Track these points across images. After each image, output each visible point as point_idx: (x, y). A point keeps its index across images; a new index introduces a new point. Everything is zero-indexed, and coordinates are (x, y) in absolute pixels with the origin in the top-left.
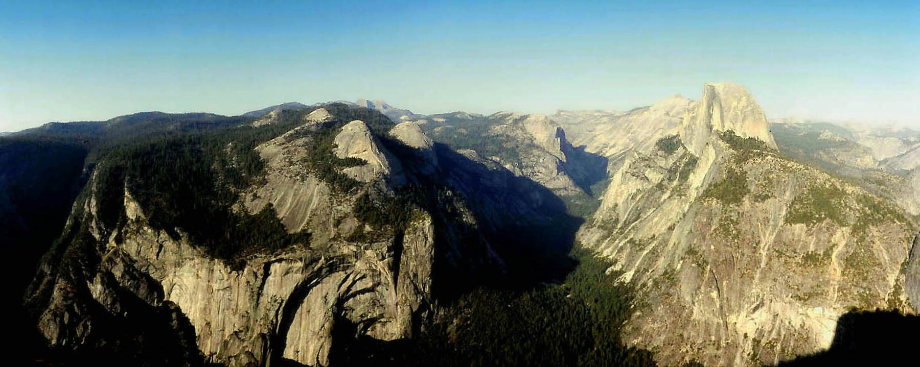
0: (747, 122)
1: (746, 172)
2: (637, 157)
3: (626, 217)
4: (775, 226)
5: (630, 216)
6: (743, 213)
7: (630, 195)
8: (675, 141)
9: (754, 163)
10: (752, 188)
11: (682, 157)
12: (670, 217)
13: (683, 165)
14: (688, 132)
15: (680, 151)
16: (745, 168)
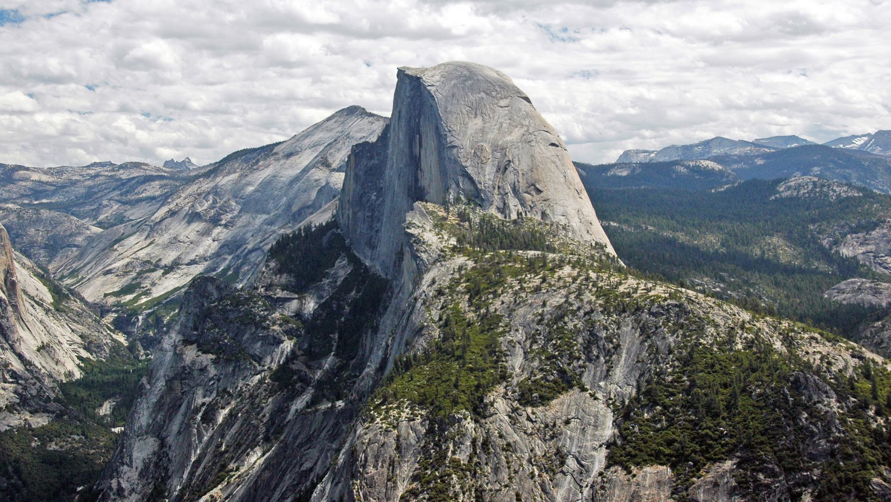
0: (510, 177)
1: (499, 318)
2: (216, 295)
3: (185, 476)
4: (584, 470)
5: (200, 470)
6: (485, 444)
7: (197, 410)
8: (325, 240)
9: (522, 289)
10: (516, 363)
11: (347, 285)
12: (307, 465)
13: (347, 309)
14: (360, 214)
15: (341, 269)
16: (496, 306)
